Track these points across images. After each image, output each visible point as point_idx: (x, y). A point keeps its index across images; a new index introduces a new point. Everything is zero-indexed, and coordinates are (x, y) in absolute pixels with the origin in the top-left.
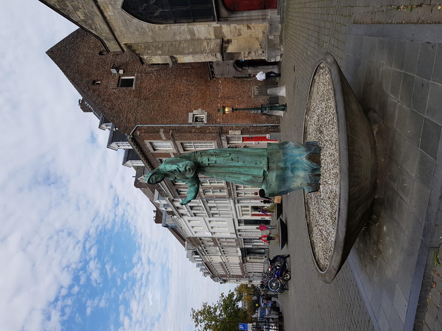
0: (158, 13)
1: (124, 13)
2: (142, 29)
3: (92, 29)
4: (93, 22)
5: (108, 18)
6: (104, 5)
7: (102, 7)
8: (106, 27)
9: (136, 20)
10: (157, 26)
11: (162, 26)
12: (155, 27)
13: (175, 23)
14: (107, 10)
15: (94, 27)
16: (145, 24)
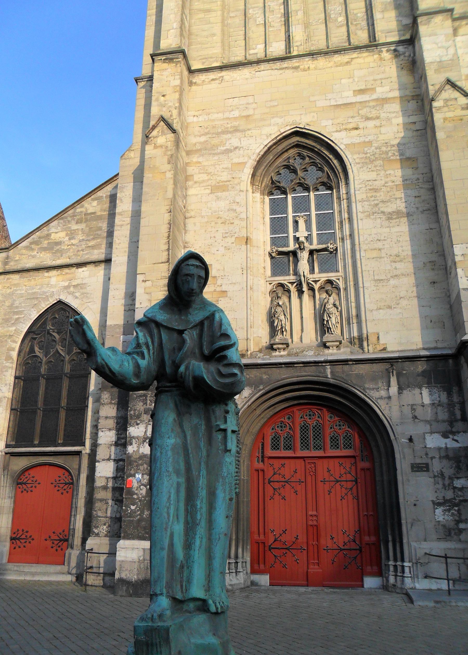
0: (38, 354)
1: (52, 301)
2: (17, 319)
3: (31, 243)
4: (45, 249)
5: (46, 274)
6: (68, 276)
7: (66, 270)
8: (30, 264)
9: (35, 315)
10: (17, 346)
11: (14, 354)
12: (15, 342)
13: (16, 378)
14: (61, 278)
15: (33, 246)
16: (25, 328)
